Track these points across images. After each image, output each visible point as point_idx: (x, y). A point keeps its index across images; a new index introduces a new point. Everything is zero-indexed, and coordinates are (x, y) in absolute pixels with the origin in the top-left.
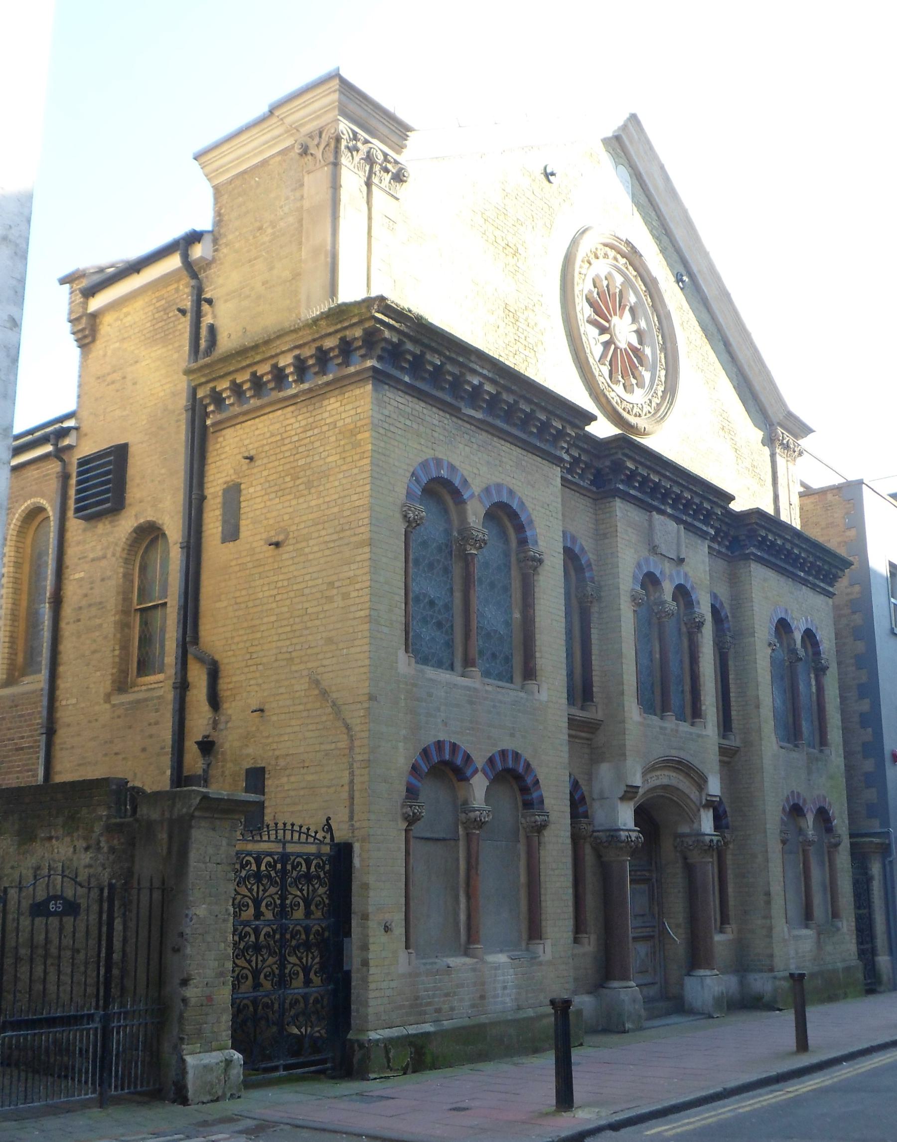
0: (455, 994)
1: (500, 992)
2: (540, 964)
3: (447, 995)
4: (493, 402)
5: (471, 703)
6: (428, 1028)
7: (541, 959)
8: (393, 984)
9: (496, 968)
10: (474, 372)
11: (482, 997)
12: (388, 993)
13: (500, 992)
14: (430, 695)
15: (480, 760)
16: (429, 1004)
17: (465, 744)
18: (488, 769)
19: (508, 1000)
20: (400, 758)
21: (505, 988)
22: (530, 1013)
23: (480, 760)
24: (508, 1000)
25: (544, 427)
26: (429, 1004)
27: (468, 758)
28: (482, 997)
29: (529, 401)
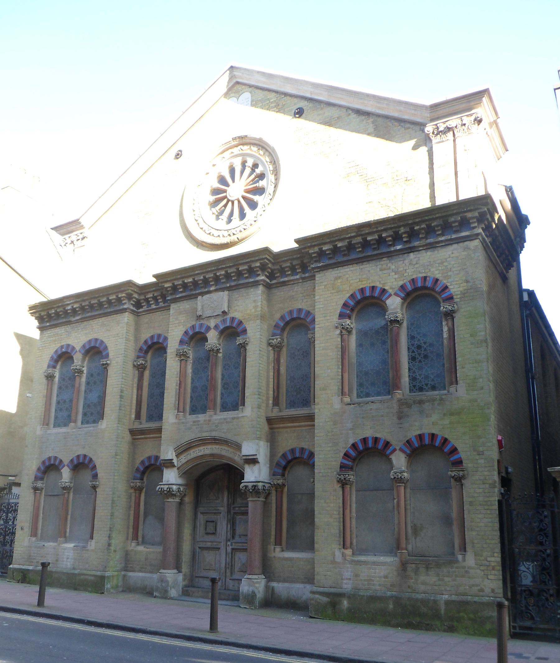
0: (45, 557)
1: (65, 560)
2: (88, 550)
3: (42, 557)
4: (82, 308)
5: (65, 438)
6: (31, 568)
7: (88, 548)
8: (22, 549)
9: (64, 549)
10: (68, 305)
11: (57, 560)
12: (20, 552)
13: (65, 560)
14: (48, 439)
15: (66, 461)
16: (34, 559)
17: (60, 456)
18: (69, 465)
19: (69, 564)
20: (32, 465)
21: (68, 558)
22: (76, 572)
23: (66, 461)
24: (69, 564)
25: (109, 302)
26: (34, 559)
27: (61, 461)
28: (57, 560)
29: (95, 298)
